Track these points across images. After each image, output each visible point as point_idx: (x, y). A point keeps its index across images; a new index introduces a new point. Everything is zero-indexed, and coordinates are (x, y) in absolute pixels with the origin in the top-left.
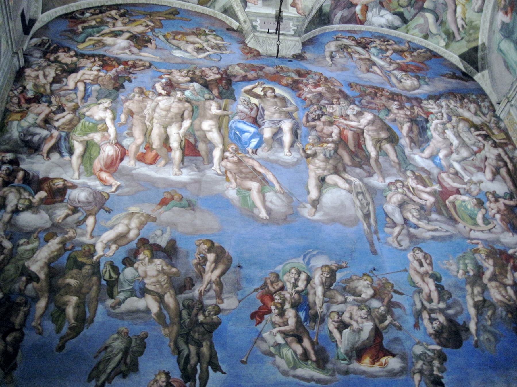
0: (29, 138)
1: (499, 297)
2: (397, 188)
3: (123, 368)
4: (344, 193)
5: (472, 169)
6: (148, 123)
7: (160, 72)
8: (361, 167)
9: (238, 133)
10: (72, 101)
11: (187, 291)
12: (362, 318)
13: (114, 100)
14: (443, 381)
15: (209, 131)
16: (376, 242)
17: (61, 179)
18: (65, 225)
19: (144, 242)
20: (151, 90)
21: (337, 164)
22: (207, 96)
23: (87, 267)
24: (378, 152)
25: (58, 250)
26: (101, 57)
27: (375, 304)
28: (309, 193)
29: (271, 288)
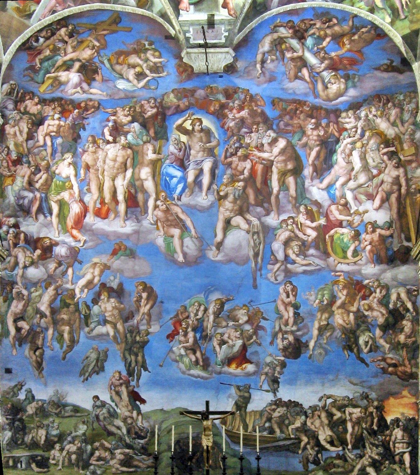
0: (21, 202)
1: (341, 322)
3: (96, 369)
4: (243, 233)
5: (363, 197)
6: (101, 177)
7: (107, 112)
8: (262, 206)
9: (168, 179)
10: (43, 160)
11: (130, 320)
13: (74, 155)
14: (279, 380)
15: (146, 180)
16: (258, 278)
19: (103, 285)
21: (244, 203)
22: (145, 138)
23: (72, 306)
24: (280, 187)
25: (55, 295)
26: (60, 99)
27: (247, 327)
28: (216, 236)
29: (181, 317)
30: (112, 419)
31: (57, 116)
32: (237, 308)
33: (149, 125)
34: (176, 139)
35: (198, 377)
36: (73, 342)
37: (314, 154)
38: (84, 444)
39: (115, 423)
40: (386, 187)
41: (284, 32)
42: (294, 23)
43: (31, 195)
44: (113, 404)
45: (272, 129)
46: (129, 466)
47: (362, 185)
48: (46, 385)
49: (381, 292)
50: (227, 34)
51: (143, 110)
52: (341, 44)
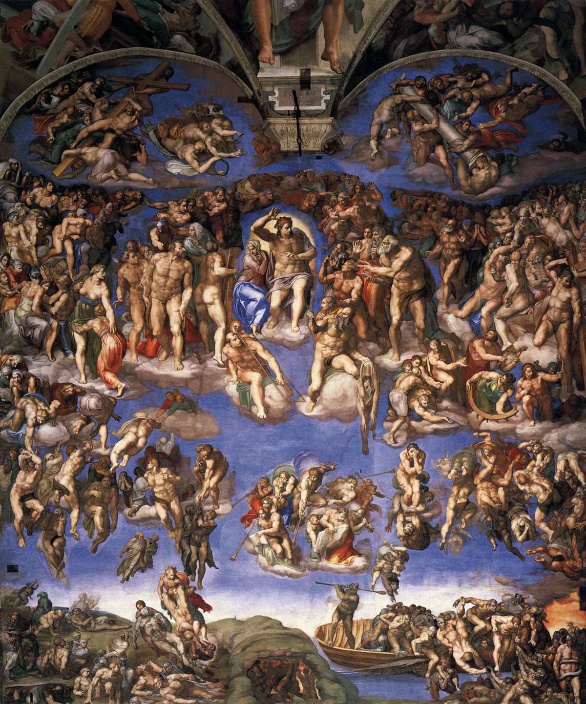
0: (30, 333)
1: (485, 499)
2: (412, 367)
4: (349, 379)
5: (520, 329)
6: (146, 299)
7: (155, 207)
8: (376, 341)
9: (242, 302)
10: (62, 274)
12: (339, 521)
13: (108, 266)
14: (399, 578)
15: (212, 304)
16: (370, 439)
17: (70, 384)
18: (82, 436)
20: (146, 243)
21: (350, 338)
22: (209, 245)
23: (106, 479)
25: (79, 463)
26: (84, 187)
27: (355, 507)
28: (310, 382)
29: (261, 493)
30: (164, 633)
31: (80, 211)
32: (340, 480)
33: (216, 226)
34: (255, 247)
35: (285, 574)
36: (108, 528)
37: (450, 268)
38: (123, 668)
39: (167, 638)
40: (553, 314)
41: (410, 94)
42: (425, 80)
43: (44, 324)
44: (165, 613)
45: (392, 234)
46: (187, 698)
47: (519, 311)
48: (68, 587)
49: (543, 459)
50: (328, 97)
51: (206, 205)
52: (494, 111)
